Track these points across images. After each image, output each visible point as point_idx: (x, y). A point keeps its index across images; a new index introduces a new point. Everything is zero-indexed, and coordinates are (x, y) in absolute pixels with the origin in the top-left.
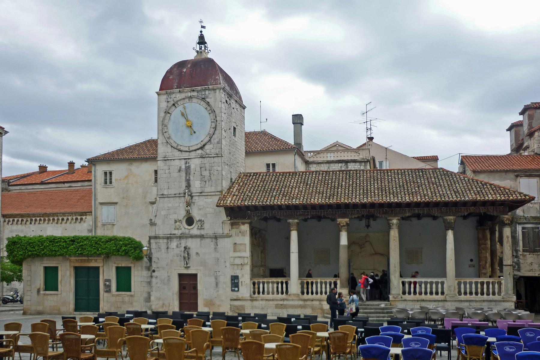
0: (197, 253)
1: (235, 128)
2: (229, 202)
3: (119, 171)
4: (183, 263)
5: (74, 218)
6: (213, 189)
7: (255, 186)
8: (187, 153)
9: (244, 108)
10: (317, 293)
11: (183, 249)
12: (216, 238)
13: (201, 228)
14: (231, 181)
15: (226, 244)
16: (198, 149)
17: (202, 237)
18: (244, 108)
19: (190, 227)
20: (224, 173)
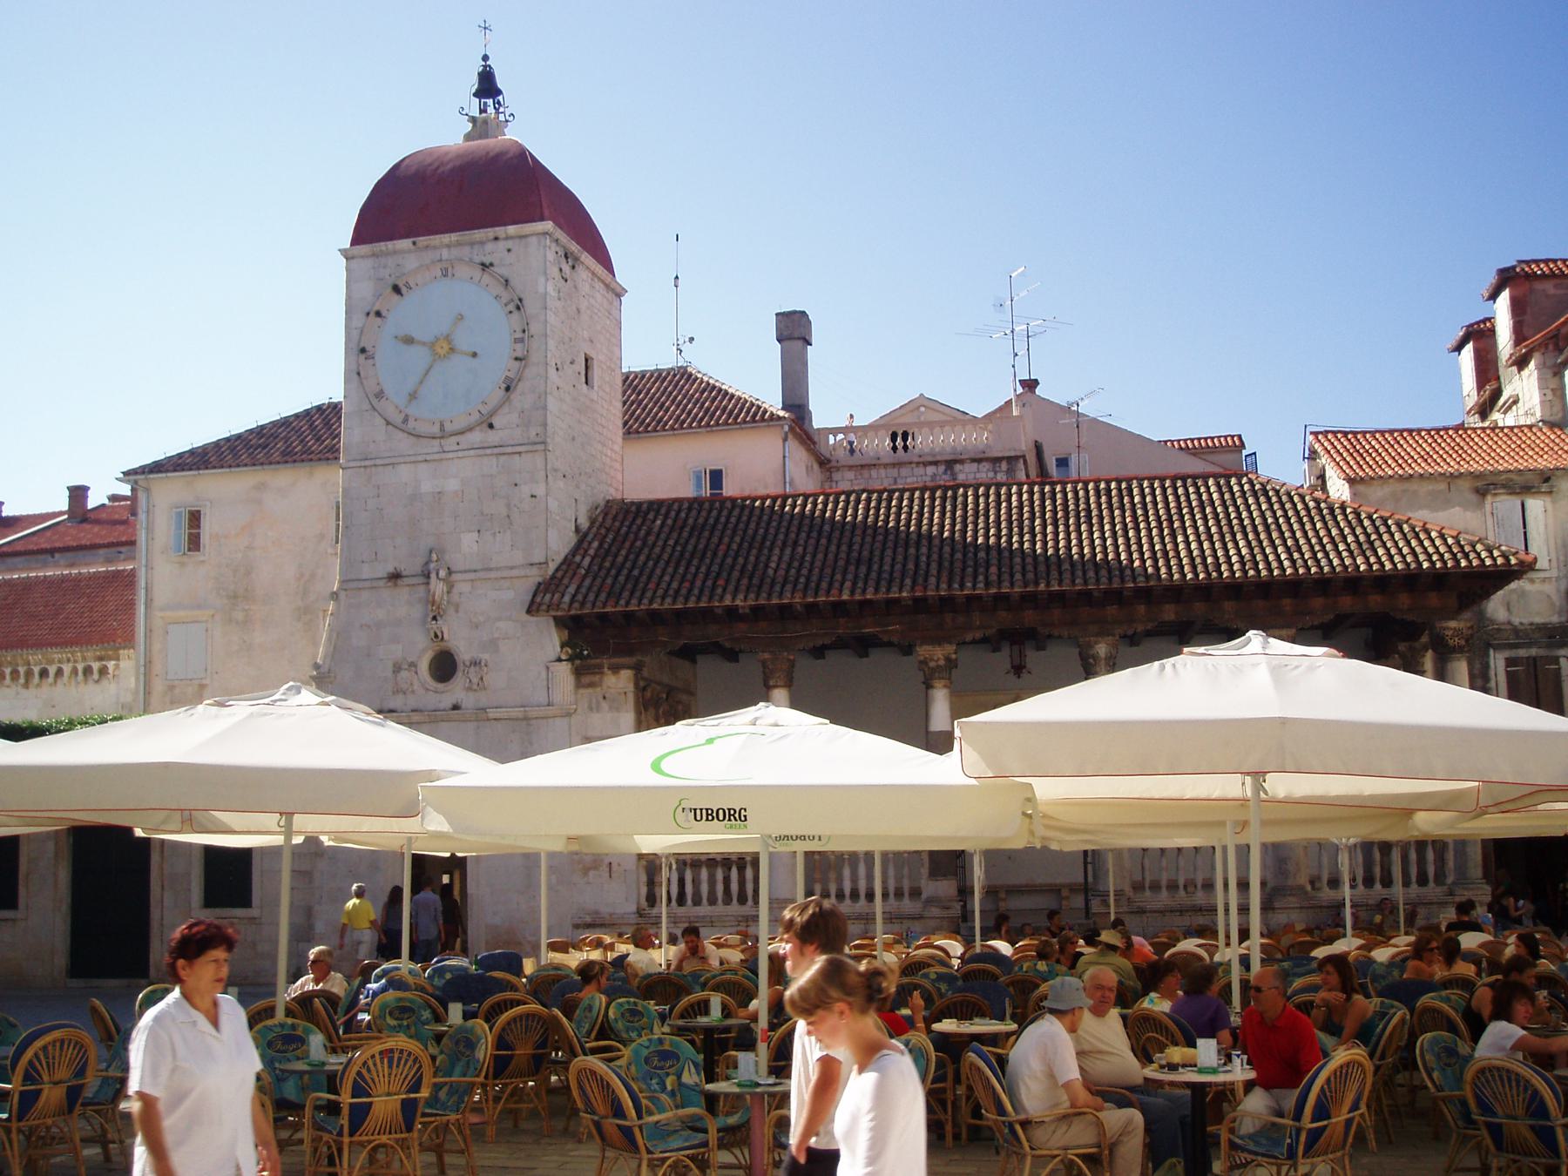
5: (80, 667)
6: (518, 558)
7: (654, 545)
9: (619, 296)
14: (577, 530)
16: (470, 429)
18: (619, 293)
19: (441, 686)
20: (553, 505)
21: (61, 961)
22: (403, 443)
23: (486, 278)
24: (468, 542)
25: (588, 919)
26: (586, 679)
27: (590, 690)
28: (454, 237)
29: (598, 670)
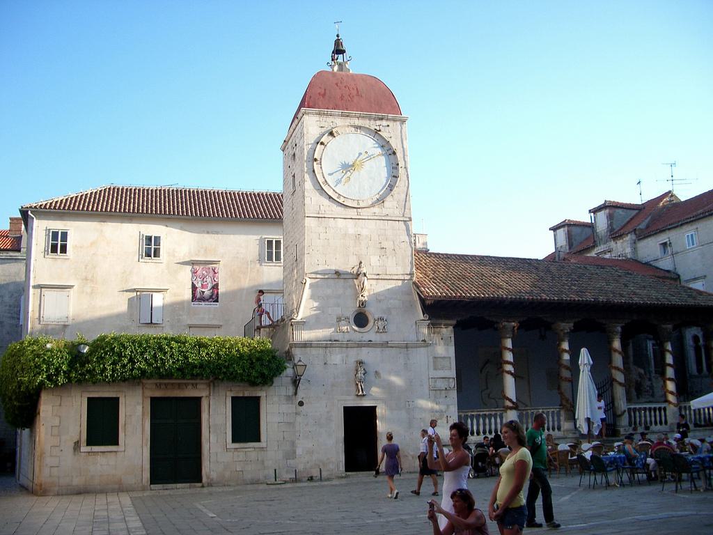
0: (376, 372)
2: (433, 291)
3: (78, 231)
8: (355, 210)
10: (661, 423)
11: (352, 365)
12: (407, 347)
15: (420, 357)
17: (385, 345)
19: (362, 330)
21: (147, 475)
24: (374, 260)
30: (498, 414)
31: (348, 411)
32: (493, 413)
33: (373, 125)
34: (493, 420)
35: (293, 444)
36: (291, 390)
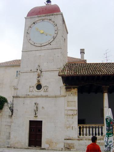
0: (43, 107)
1: (65, 39)
4: (33, 113)
8: (40, 47)
11: (34, 104)
13: (46, 91)
15: (62, 101)
17: (47, 96)
22: (34, 48)
23: (50, 21)
25: (68, 138)
26: (68, 90)
27: (69, 92)
28: (45, 15)
29: (70, 88)
30: (100, 126)
31: (31, 122)
32: (97, 126)
33: (49, 18)
34: (97, 129)
35: (10, 133)
36: (11, 114)
